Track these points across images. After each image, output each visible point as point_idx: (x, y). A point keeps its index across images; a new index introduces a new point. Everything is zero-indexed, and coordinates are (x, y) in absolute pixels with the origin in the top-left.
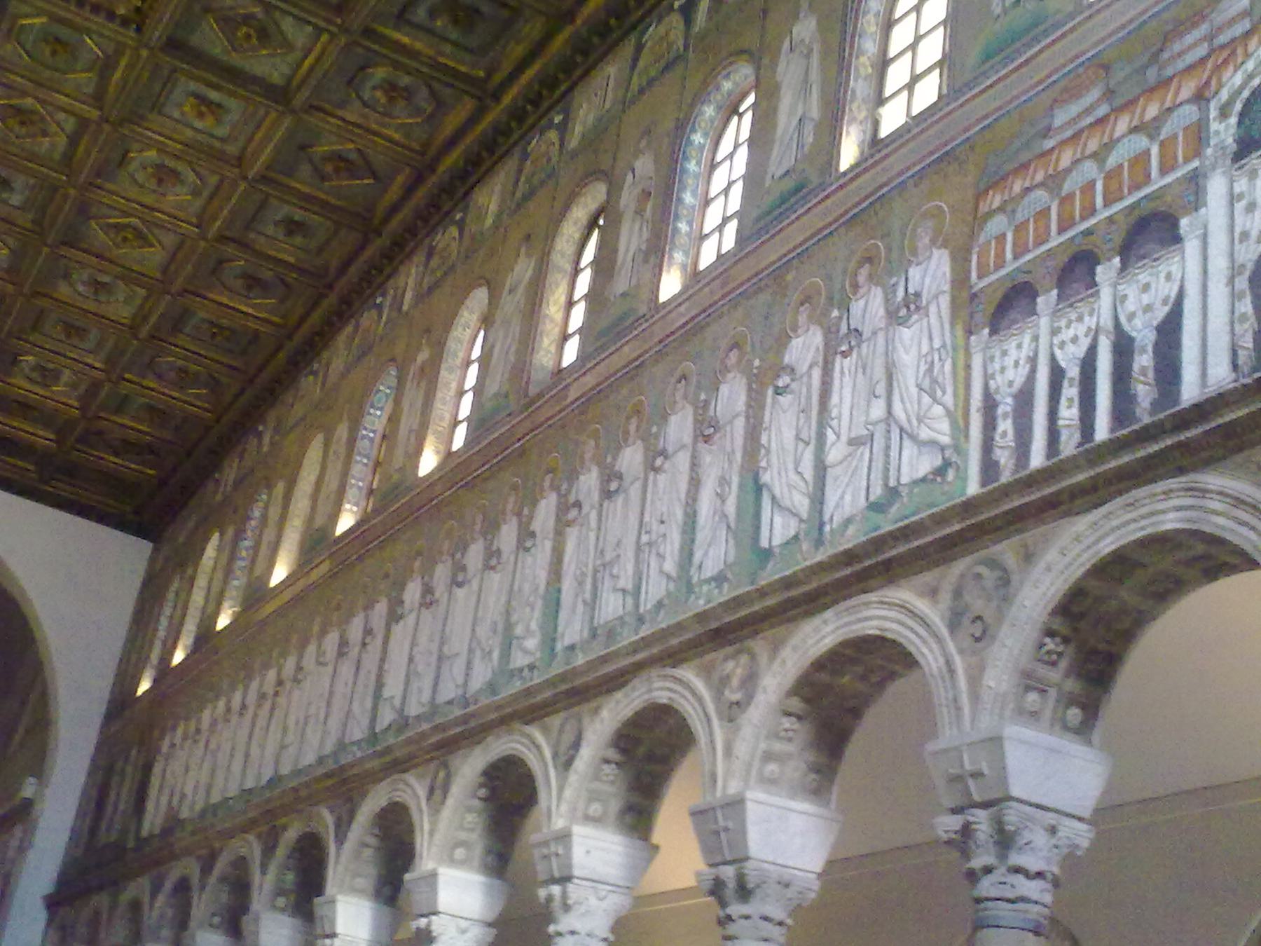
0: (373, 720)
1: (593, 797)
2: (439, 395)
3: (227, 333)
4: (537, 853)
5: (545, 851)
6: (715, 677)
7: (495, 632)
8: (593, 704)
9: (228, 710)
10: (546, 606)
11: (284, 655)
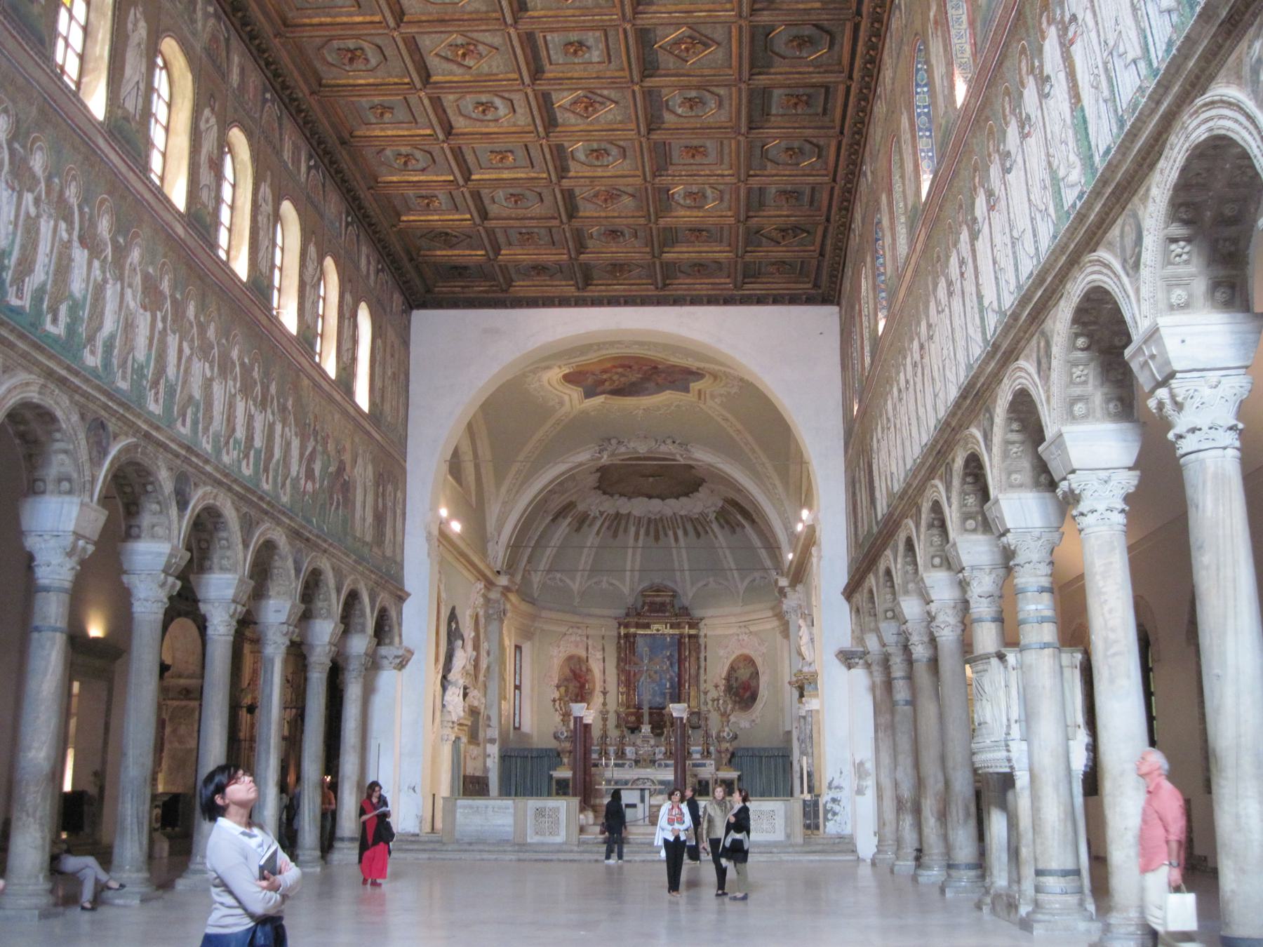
0: (984, 333)
1: (1172, 283)
2: (953, 32)
3: (805, 98)
4: (1135, 366)
5: (1141, 359)
6: (1246, 70)
7: (1045, 188)
8: (1142, 191)
9: (900, 391)
10: (1076, 133)
11: (919, 324)
